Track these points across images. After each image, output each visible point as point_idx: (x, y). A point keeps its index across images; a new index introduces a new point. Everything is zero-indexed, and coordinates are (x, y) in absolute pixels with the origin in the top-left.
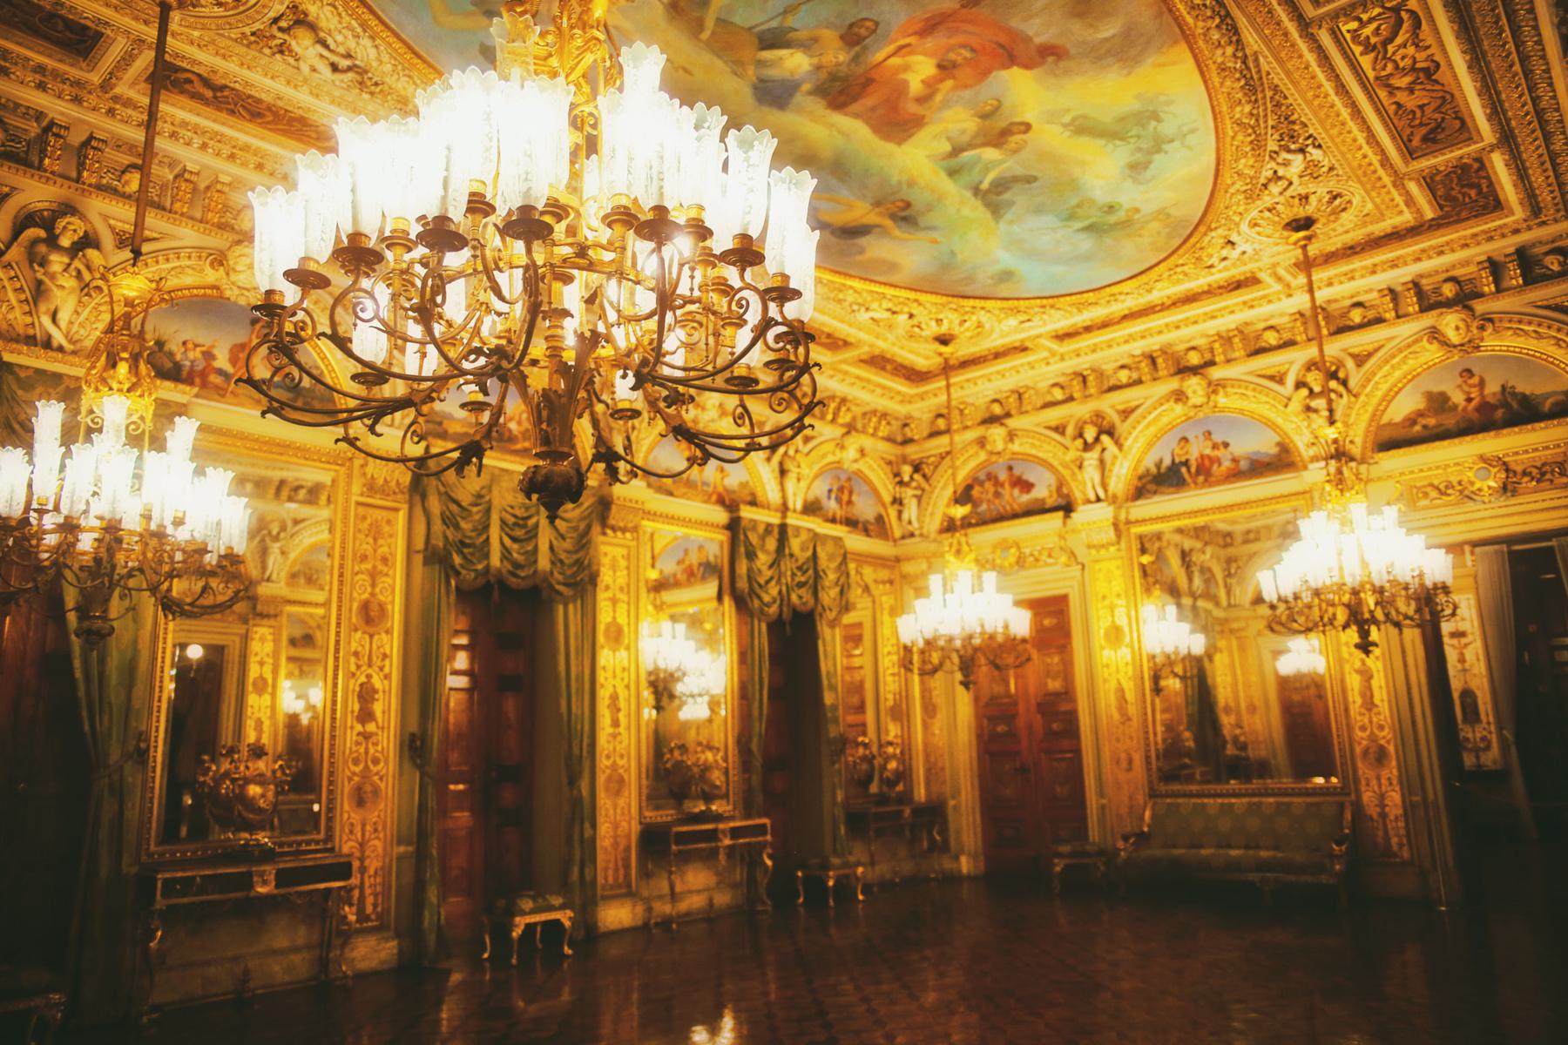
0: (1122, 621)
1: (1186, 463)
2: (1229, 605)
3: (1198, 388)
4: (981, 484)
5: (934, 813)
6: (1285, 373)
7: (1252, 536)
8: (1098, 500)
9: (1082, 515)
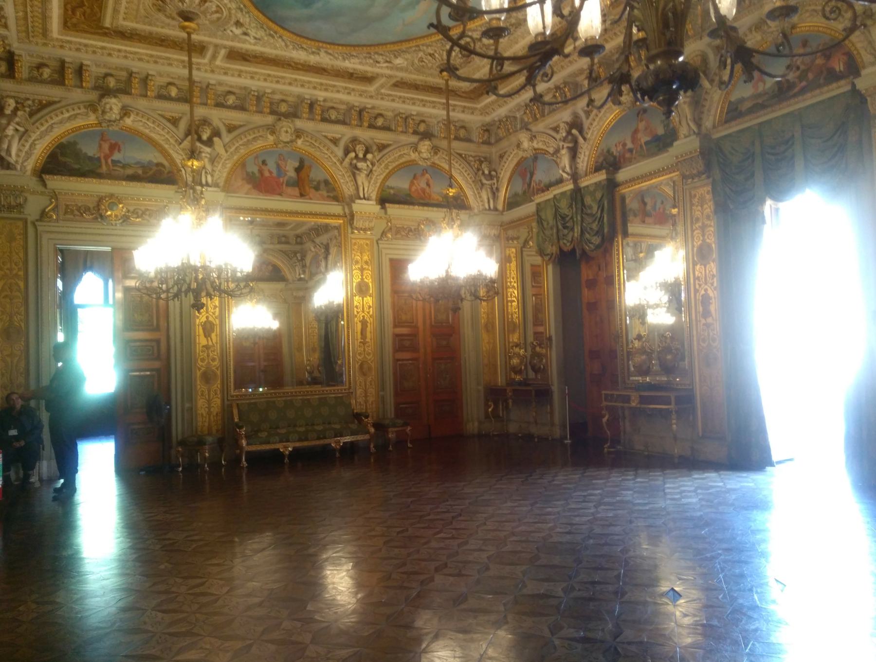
6: (340, 139)
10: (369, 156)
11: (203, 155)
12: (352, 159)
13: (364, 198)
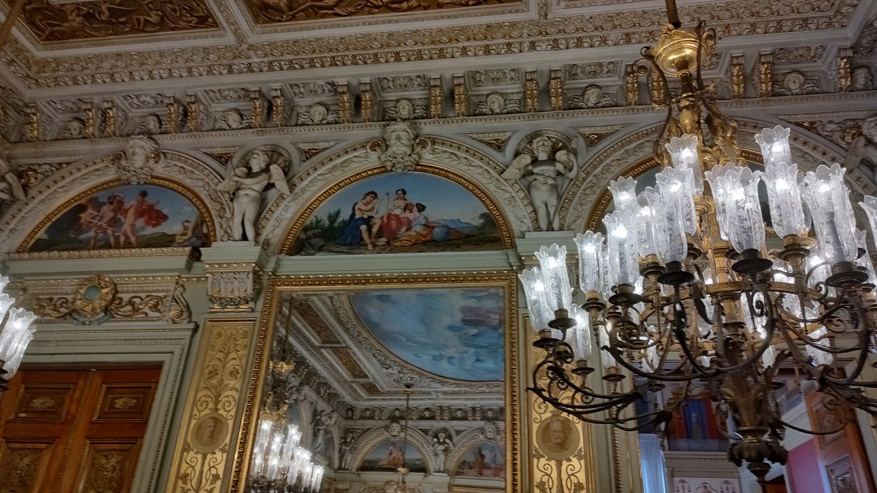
0: (228, 412)
1: (368, 221)
2: (340, 468)
3: (403, 135)
4: (97, 204)
7: (368, 413)
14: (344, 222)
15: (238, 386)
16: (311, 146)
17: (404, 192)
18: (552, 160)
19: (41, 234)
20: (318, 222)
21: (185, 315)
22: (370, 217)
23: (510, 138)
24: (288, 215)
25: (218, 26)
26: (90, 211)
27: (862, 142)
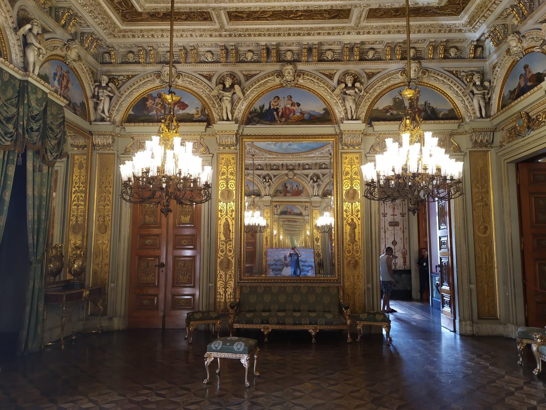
1: (277, 110)
4: (154, 99)
5: (100, 291)
8: (228, 120)
9: (218, 126)
10: (357, 85)
11: (225, 98)
12: (343, 89)
13: (352, 119)
14: (266, 110)
15: (234, 178)
16: (248, 73)
17: (291, 97)
18: (353, 86)
19: (131, 112)
20: (255, 110)
21: (207, 150)
22: (278, 108)
23: (335, 73)
24: (243, 108)
25: (211, 20)
26: (150, 101)
27: (472, 84)
